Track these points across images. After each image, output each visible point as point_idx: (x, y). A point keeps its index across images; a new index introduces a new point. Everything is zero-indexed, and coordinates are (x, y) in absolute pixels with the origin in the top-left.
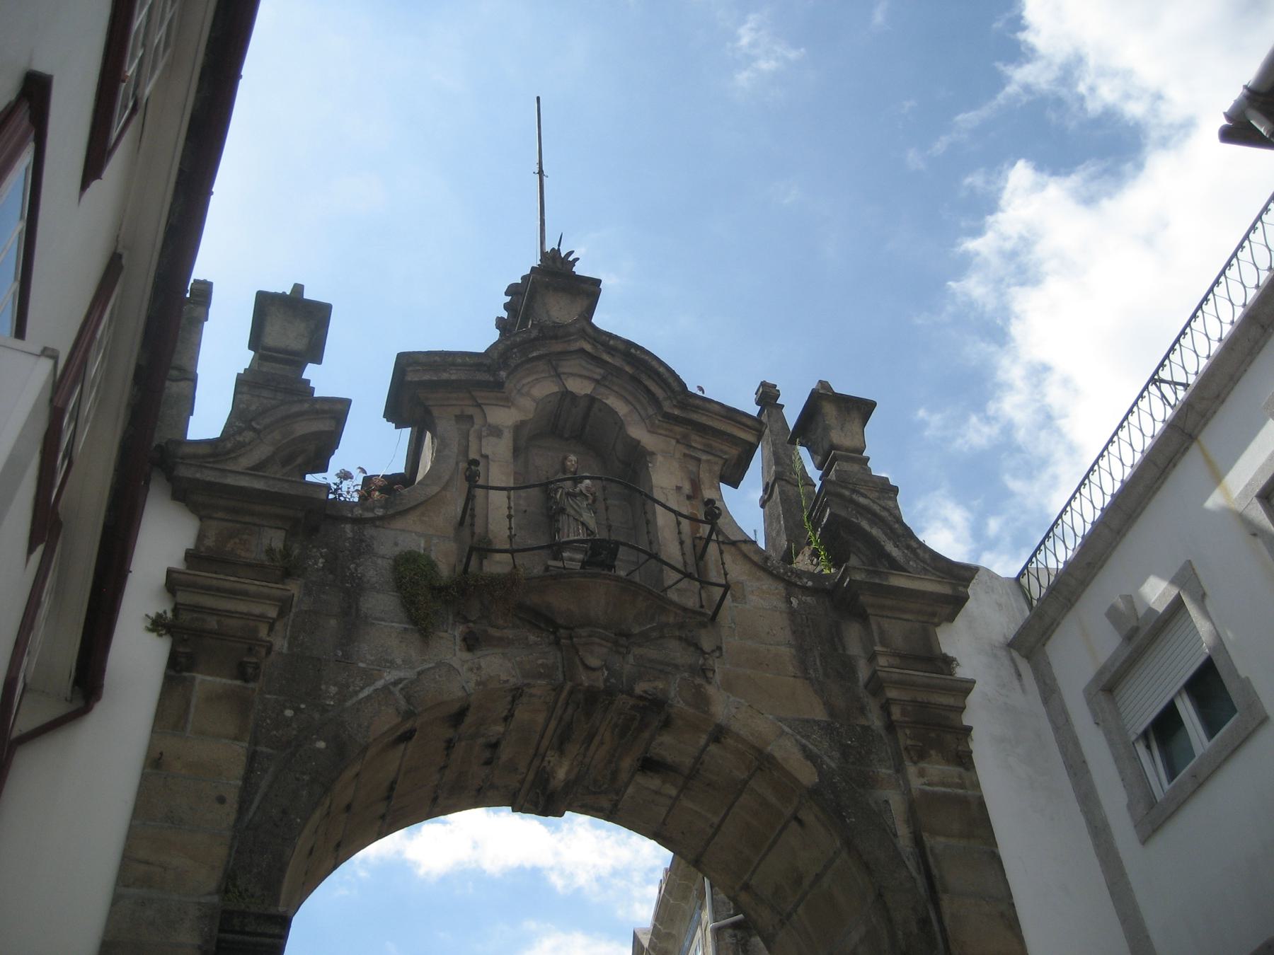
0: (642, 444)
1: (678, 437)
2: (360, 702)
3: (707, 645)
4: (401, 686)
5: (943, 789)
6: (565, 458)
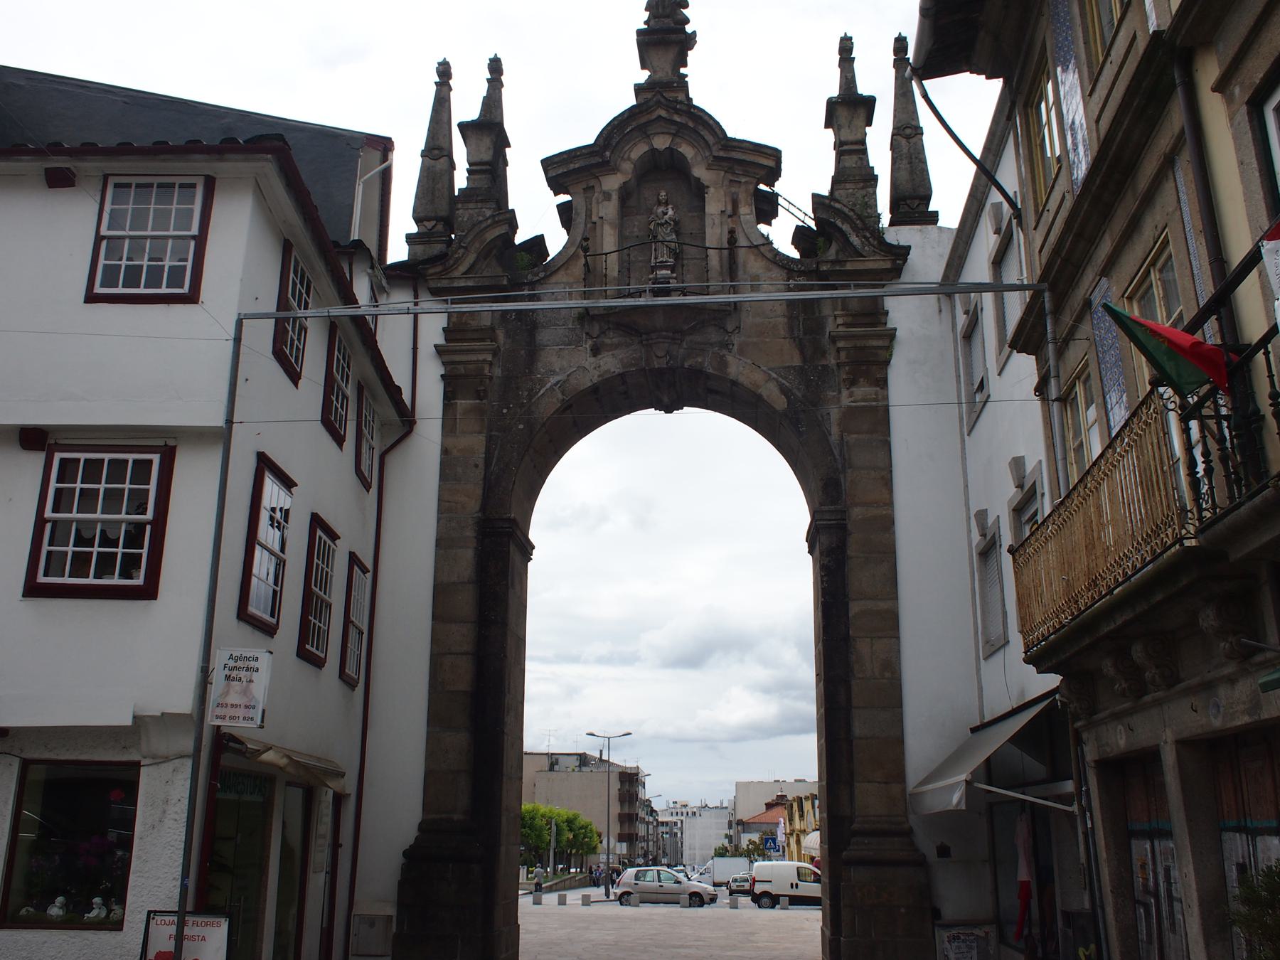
0: (701, 181)
1: (726, 169)
2: (538, 398)
3: (730, 328)
4: (559, 385)
5: (863, 404)
6: (659, 195)
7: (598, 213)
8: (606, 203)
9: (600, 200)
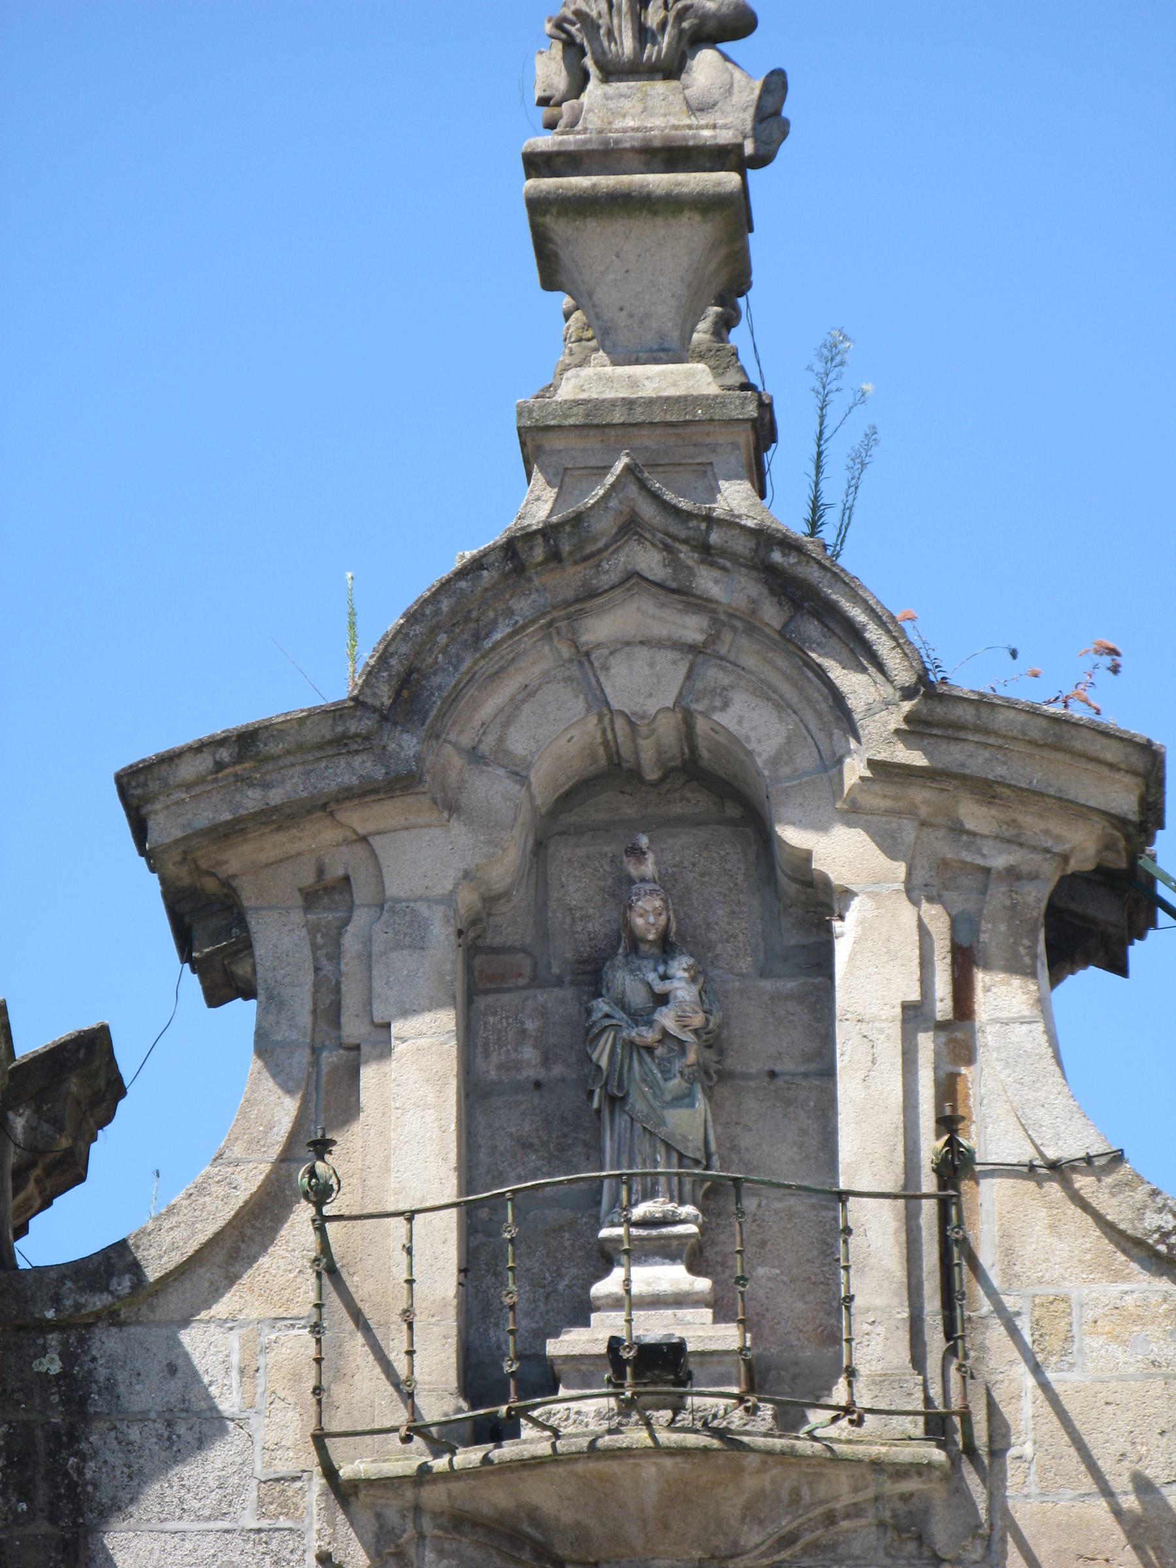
7: (369, 1002)
8: (403, 961)
9: (376, 948)
